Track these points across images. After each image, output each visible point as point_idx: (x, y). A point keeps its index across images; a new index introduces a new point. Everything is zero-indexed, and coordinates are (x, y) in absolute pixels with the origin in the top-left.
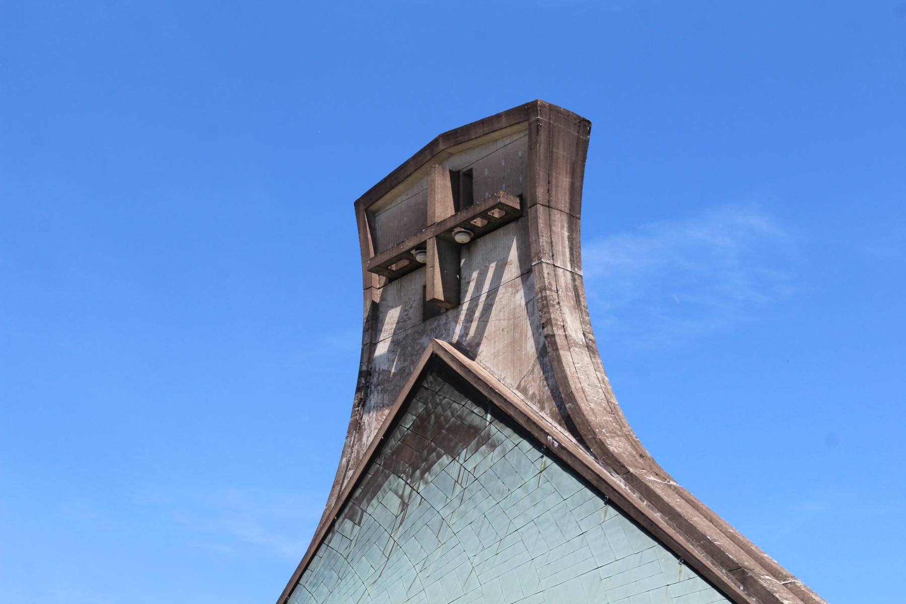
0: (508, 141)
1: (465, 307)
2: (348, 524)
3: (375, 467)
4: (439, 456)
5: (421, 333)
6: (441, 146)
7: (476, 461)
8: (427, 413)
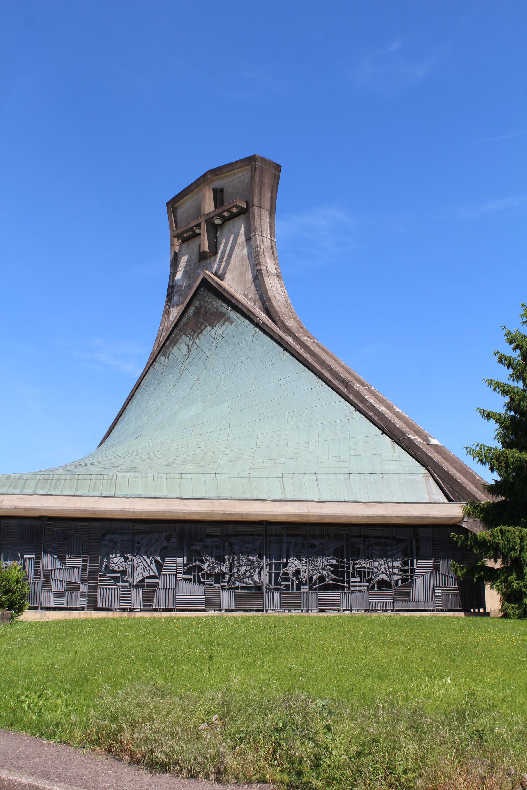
0: (241, 174)
1: (219, 255)
2: (163, 358)
3: (176, 331)
4: (206, 327)
5: (198, 268)
6: (209, 176)
7: (223, 329)
8: (200, 307)
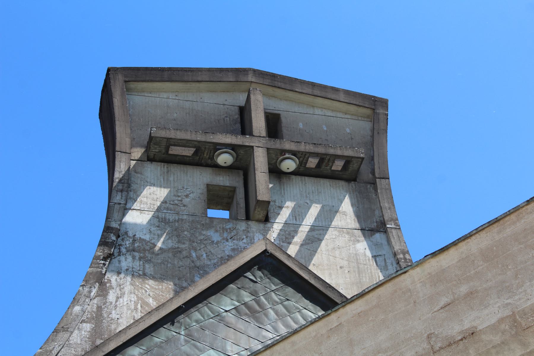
0: (329, 113)
